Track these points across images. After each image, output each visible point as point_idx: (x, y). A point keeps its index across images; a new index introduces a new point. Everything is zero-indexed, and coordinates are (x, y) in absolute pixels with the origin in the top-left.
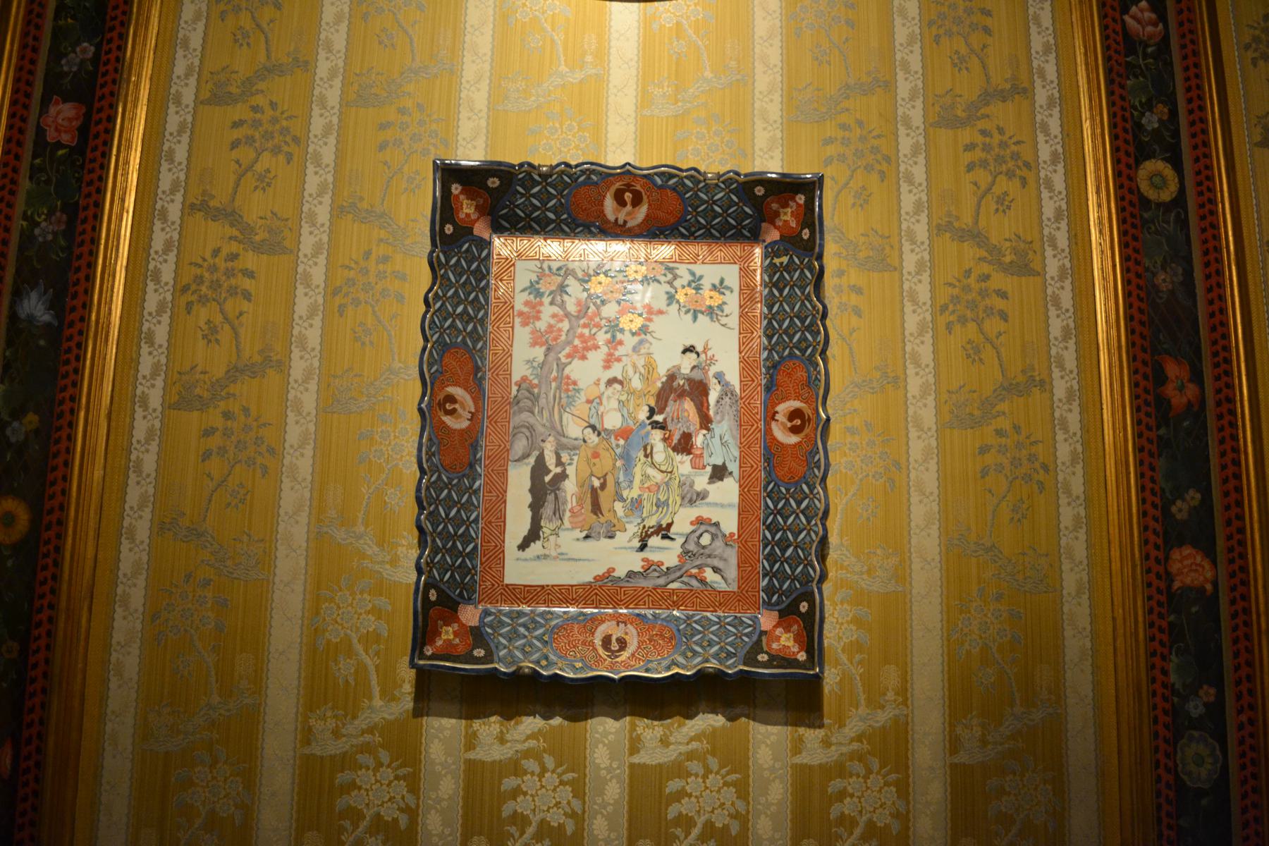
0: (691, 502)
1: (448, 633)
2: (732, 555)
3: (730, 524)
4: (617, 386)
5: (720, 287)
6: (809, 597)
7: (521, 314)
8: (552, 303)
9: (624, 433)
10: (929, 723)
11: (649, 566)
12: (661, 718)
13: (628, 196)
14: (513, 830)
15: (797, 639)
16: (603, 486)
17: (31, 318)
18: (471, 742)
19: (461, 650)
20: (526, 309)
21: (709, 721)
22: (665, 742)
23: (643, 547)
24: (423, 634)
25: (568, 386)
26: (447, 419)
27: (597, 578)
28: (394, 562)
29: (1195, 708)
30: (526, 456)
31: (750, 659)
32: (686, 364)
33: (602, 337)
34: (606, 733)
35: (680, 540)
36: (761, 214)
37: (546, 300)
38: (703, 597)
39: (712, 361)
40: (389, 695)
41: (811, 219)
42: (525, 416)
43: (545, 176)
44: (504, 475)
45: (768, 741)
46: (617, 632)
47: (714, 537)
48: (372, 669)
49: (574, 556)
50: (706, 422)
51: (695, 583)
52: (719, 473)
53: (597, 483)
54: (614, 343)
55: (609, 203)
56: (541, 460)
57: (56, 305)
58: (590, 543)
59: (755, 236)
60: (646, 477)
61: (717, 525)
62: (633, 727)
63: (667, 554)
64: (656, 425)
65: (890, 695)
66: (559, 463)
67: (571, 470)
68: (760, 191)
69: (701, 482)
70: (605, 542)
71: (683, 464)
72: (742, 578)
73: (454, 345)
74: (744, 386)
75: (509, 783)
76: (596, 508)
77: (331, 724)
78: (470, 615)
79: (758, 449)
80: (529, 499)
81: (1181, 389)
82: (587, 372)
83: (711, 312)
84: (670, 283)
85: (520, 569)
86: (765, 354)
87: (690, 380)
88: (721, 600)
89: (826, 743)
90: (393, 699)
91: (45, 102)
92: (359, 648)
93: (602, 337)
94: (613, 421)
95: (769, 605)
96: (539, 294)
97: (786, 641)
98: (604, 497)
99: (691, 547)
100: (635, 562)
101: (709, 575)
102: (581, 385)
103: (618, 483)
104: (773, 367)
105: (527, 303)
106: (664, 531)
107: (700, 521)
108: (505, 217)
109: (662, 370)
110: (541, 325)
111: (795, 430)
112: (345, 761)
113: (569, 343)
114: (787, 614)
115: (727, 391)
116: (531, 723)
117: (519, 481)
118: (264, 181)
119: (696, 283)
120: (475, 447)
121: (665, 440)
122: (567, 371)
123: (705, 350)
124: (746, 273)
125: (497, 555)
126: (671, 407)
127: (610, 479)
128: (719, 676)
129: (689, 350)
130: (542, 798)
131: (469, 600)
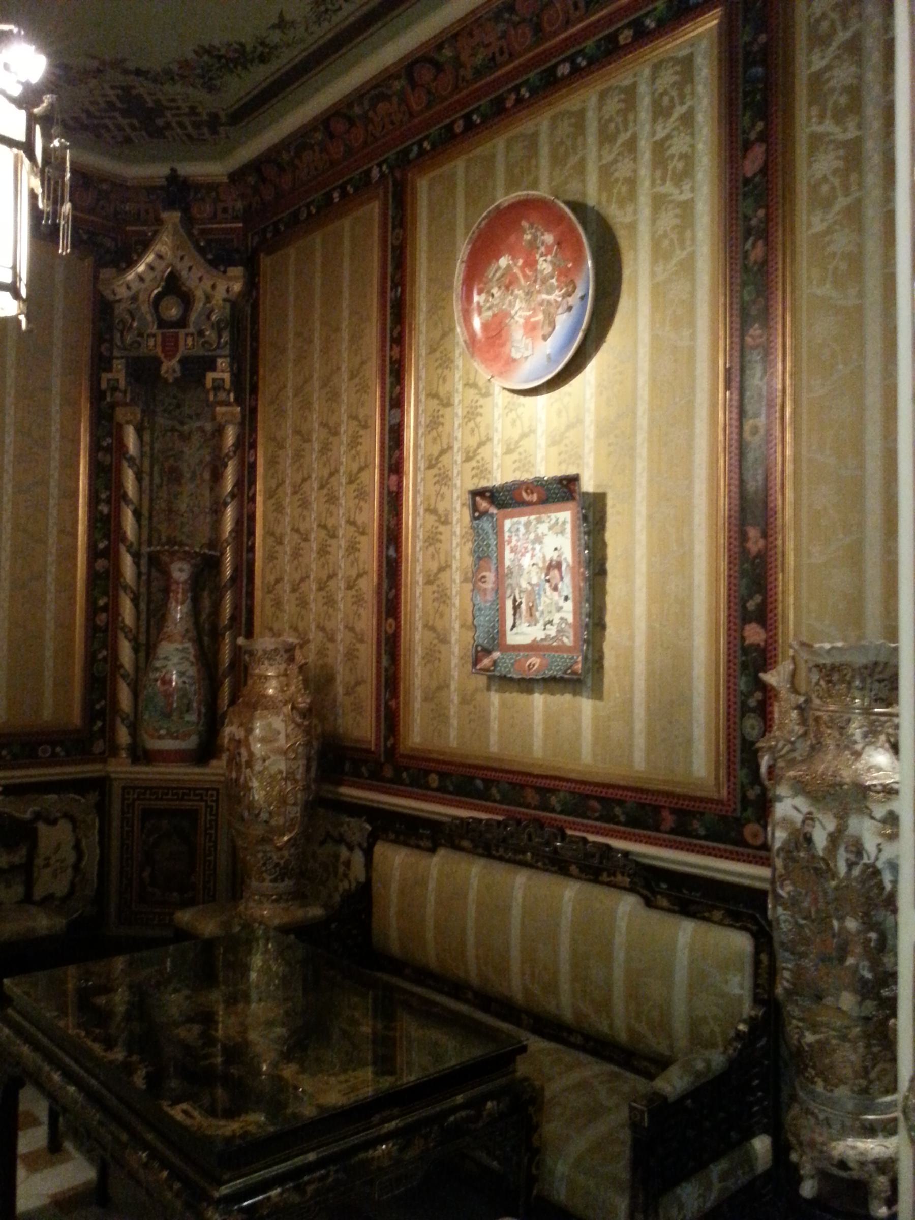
3: (570, 619)
5: (564, 522)
9: (538, 585)
11: (547, 636)
21: (568, 697)
24: (476, 662)
25: (520, 566)
29: (752, 703)
31: (565, 672)
32: (555, 555)
34: (539, 700)
38: (562, 648)
45: (586, 705)
49: (522, 634)
50: (562, 578)
52: (566, 599)
54: (533, 549)
55: (524, 495)
63: (552, 631)
64: (548, 581)
67: (523, 601)
69: (561, 603)
72: (575, 641)
76: (531, 615)
78: (496, 655)
81: (756, 542)
82: (526, 561)
85: (513, 638)
93: (530, 547)
101: (565, 640)
106: (550, 622)
107: (562, 618)
109: (548, 559)
117: (509, 604)
118: (443, 497)
125: (504, 635)
126: (551, 573)
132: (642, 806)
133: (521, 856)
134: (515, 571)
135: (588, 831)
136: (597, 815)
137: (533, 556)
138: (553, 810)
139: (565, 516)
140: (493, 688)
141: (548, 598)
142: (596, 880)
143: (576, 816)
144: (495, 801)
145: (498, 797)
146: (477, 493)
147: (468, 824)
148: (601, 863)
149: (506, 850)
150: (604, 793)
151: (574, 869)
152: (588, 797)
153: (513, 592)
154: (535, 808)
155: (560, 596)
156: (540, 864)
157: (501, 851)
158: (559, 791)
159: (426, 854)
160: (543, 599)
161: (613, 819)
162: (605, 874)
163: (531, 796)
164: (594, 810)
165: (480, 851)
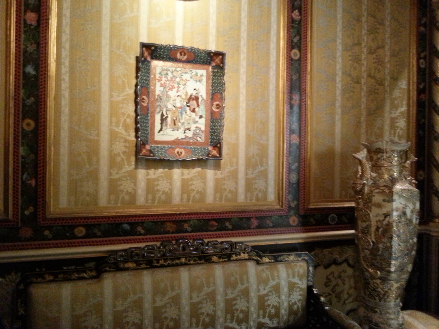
0: (195, 123)
1: (144, 151)
2: (203, 135)
3: (203, 128)
4: (179, 97)
5: (202, 76)
6: (220, 143)
7: (158, 79)
8: (165, 77)
9: (181, 108)
10: (242, 169)
11: (186, 137)
12: (188, 169)
13: (183, 53)
14: (158, 193)
15: (217, 152)
16: (176, 119)
17: (29, 73)
18: (148, 174)
19: (147, 154)
20: (159, 78)
21: (198, 170)
22: (189, 174)
23: (185, 133)
25: (168, 96)
26: (143, 104)
27: (175, 139)
28: (129, 135)
30: (159, 112)
32: (194, 93)
33: (176, 85)
34: (177, 172)
35: (193, 131)
36: (213, 60)
37: (163, 76)
38: (197, 143)
39: (200, 92)
40: (129, 165)
41: (223, 61)
42: (159, 103)
43: (165, 48)
44: (154, 116)
45: (210, 174)
46: (180, 150)
47: (200, 131)
48: (125, 159)
50: (198, 106)
51: (195, 140)
52: (201, 117)
53: (175, 119)
54: (179, 87)
56: (162, 113)
57: (37, 69)
58: (174, 132)
59: (210, 64)
60: (185, 117)
61: (200, 128)
62: (182, 170)
63: (190, 134)
64: (188, 106)
65: (234, 164)
66: (167, 114)
67: (169, 116)
68: (212, 54)
69: (197, 119)
70: (177, 131)
71: (193, 115)
72: (205, 140)
73: (144, 86)
74: (207, 98)
75: (156, 183)
76: (175, 124)
77: (116, 171)
78: (148, 147)
79: (209, 112)
80: (160, 122)
82: (173, 94)
83: (200, 81)
84: (191, 74)
85: (158, 137)
86: (211, 91)
87: (195, 96)
88: (201, 144)
89: (221, 174)
90: (131, 166)
91: (25, 12)
92: (122, 155)
93: (176, 85)
94: (178, 105)
95: (211, 145)
96: (162, 75)
97: (215, 152)
98: (176, 122)
99: (195, 133)
100: (183, 136)
101: (199, 139)
102: (171, 97)
103: (179, 119)
104: (213, 94)
105: (159, 77)
106: (189, 129)
107: (197, 127)
108: (155, 56)
110: (162, 82)
111: (217, 108)
112: (119, 179)
113: (168, 87)
114: (215, 147)
115: (203, 99)
116: (161, 170)
117: (158, 118)
119: (196, 74)
120: (148, 110)
121: (190, 109)
122: (168, 93)
123: (199, 89)
124: (207, 72)
125: (153, 134)
127: (178, 118)
128: (202, 159)
129: (195, 89)
130: (163, 186)
131: (148, 144)
132: (241, 219)
133: (177, 261)
134: (164, 98)
135: (217, 237)
136: (215, 228)
137: (178, 91)
138: (187, 231)
139: (203, 72)
140: (140, 167)
141: (188, 115)
142: (229, 260)
143: (202, 232)
144: (141, 234)
145: (142, 231)
146: (144, 46)
147: (132, 252)
148: (232, 250)
149: (165, 260)
150: (218, 216)
151: (215, 258)
152: (210, 220)
153: (161, 110)
154: (173, 233)
155: (196, 115)
156: (192, 262)
157: (162, 262)
158: (190, 220)
159: (97, 280)
160: (184, 115)
161: (226, 229)
162: (234, 256)
163: (170, 227)
164: (212, 226)
165: (144, 266)
